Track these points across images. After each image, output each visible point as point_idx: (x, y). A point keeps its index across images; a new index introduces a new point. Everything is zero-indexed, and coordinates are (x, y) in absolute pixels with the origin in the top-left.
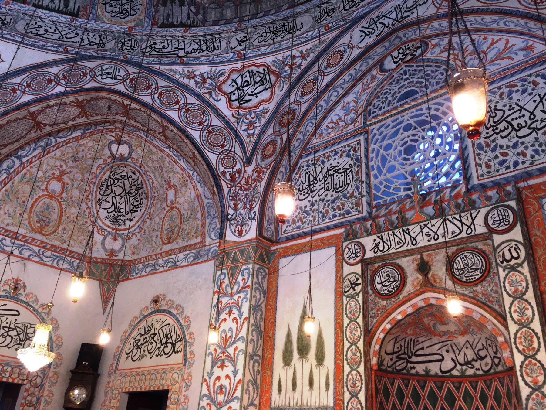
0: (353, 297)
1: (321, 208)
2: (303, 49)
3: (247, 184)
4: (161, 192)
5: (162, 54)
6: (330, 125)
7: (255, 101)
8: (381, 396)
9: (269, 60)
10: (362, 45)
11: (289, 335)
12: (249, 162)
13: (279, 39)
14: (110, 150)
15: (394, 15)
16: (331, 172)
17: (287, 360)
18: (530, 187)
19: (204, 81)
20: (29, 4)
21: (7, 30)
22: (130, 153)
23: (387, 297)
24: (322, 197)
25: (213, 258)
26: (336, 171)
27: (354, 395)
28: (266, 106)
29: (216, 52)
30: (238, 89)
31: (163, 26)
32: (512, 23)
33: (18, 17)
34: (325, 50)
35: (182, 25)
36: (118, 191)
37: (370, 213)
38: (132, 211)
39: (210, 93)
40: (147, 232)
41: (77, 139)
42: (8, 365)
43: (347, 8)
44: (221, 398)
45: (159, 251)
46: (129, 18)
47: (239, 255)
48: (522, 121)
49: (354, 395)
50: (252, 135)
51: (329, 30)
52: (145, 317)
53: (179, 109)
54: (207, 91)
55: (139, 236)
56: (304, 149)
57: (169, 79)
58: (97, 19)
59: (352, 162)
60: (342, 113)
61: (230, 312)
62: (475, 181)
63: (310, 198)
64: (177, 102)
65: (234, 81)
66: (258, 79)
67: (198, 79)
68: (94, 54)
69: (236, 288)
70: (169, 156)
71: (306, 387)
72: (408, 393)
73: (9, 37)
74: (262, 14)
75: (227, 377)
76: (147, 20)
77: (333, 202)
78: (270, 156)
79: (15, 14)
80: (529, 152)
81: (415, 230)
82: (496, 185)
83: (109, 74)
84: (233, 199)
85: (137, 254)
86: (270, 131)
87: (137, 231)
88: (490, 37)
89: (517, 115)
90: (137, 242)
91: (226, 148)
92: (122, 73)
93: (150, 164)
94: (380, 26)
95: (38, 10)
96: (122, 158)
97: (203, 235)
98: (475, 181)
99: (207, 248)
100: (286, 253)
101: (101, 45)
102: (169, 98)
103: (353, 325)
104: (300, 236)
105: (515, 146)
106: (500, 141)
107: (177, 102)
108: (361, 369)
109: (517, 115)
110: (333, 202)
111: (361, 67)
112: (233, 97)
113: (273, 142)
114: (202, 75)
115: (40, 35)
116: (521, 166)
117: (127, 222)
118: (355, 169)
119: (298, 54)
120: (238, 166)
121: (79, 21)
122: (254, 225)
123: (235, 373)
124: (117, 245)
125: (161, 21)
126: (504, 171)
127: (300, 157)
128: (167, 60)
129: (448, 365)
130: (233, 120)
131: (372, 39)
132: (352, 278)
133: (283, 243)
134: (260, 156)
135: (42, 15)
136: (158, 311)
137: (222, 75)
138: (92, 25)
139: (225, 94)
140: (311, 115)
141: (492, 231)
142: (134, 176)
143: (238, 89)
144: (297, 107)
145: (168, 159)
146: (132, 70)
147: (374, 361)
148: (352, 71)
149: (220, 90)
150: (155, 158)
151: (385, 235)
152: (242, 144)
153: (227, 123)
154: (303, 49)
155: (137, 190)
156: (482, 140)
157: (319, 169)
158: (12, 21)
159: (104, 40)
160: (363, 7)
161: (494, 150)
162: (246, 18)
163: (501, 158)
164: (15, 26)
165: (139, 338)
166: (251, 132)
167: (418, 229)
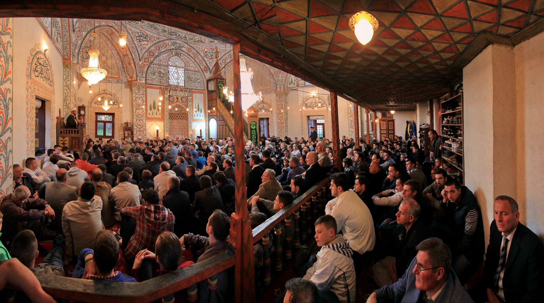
7: (143, 43)
9: (148, 33)
11: (151, 105)
12: (140, 60)
23: (172, 102)
32: (195, 63)
34: (163, 41)
44: (140, 116)
47: (140, 86)
51: (164, 36)
60: (162, 58)
61: (139, 99)
62: (186, 87)
66: (144, 36)
69: (140, 94)
71: (156, 115)
81: (178, 92)
82: (188, 89)
86: (146, 54)
88: (191, 62)
98: (186, 87)
100: (149, 87)
104: (152, 84)
123: (143, 112)
129: (173, 112)
130: (137, 46)
131: (174, 47)
134: (144, 60)
152: (139, 54)
157: (156, 70)
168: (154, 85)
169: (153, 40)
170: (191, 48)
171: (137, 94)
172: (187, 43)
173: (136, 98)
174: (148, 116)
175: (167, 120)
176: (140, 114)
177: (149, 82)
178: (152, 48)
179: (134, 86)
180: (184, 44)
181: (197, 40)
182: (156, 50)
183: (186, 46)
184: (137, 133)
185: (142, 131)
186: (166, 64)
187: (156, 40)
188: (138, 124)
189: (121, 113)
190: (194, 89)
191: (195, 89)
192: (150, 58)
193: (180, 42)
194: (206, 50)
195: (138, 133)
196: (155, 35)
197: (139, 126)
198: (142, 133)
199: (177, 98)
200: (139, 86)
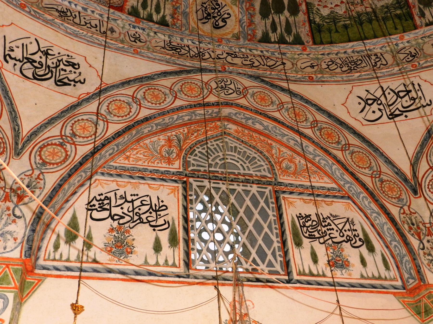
20: (421, 27)
21: (422, 59)
33: (418, 44)
73: (429, 64)
79: (414, 43)
158: (417, 50)
164: (424, 53)
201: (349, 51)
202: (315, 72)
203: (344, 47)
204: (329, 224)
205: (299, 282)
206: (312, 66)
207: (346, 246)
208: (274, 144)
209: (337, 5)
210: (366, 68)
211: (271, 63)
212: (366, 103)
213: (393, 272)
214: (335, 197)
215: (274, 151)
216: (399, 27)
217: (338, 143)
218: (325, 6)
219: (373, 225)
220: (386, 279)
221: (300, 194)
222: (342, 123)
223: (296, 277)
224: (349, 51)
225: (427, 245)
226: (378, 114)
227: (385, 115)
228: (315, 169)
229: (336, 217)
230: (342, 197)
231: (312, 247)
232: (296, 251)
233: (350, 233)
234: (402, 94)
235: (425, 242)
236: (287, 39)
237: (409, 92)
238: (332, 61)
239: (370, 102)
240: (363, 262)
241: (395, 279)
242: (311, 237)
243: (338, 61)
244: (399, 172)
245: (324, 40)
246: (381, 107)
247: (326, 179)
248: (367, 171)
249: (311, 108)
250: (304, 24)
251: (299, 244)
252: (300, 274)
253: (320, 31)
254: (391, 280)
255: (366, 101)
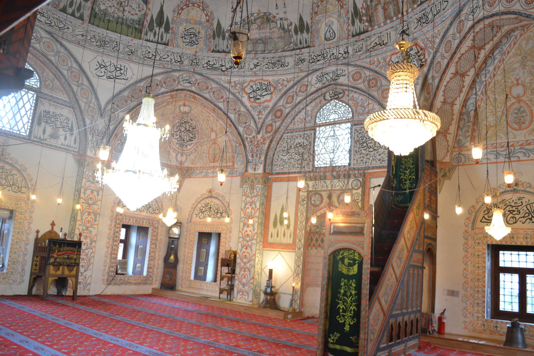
0: (303, 205)
1: (292, 162)
2: (289, 77)
3: (258, 144)
4: (207, 132)
5: (213, 68)
6: (299, 120)
7: (262, 99)
8: (310, 241)
9: (270, 79)
10: (316, 86)
11: (276, 216)
12: (259, 133)
13: (276, 69)
14: (180, 109)
15: (331, 76)
16: (298, 145)
17: (275, 225)
18: (369, 173)
19: (236, 86)
22: (190, 110)
24: (293, 157)
25: (239, 176)
26: (301, 146)
27: (300, 240)
28: (268, 104)
29: (242, 70)
30: (253, 91)
31: (213, 51)
33: (138, 47)
34: (299, 81)
35: (224, 52)
36: (183, 129)
37: (313, 170)
38: (190, 140)
39: (239, 92)
40: (199, 152)
41: (164, 106)
42: (144, 219)
43: (311, 62)
44: (248, 239)
45: (208, 165)
46: (195, 46)
48: (371, 145)
49: (300, 240)
50: (261, 118)
51: (301, 71)
52: (204, 198)
53: (223, 102)
54: (237, 91)
55: (195, 154)
56: (286, 129)
57: (217, 83)
58: (178, 46)
59: (308, 143)
62: (352, 166)
63: (287, 156)
64: (222, 98)
65: (252, 87)
66: (264, 88)
67: (233, 84)
68: (179, 69)
70: (213, 116)
71: (282, 236)
72: (320, 239)
73: (135, 61)
74: (267, 52)
75: (250, 231)
76: (205, 47)
77: (298, 160)
78: (270, 132)
80: (371, 159)
82: (358, 169)
83: (186, 80)
84: (251, 152)
85: (195, 165)
86: (270, 118)
87: (194, 151)
89: (370, 142)
90: (194, 158)
91: (247, 124)
92: (194, 80)
93: (201, 117)
94: (325, 79)
95: (148, 43)
96: (185, 113)
97: (233, 163)
99: (236, 169)
100: (276, 180)
101: (181, 62)
102: (218, 95)
103: (302, 216)
104: (282, 174)
105: (367, 155)
106: (364, 152)
107: (222, 98)
108: (303, 232)
109: (370, 142)
110: (298, 160)
111: (316, 95)
112: (251, 96)
113: (271, 125)
114: (235, 82)
115: (150, 58)
116: (367, 164)
117: (188, 146)
118: (308, 147)
119: (285, 79)
120: (253, 134)
121: (169, 48)
122: (262, 166)
123: (254, 230)
124: (184, 159)
125: (212, 49)
126: (362, 164)
127: (284, 133)
128: (216, 73)
130: (250, 109)
132: (303, 197)
133: (274, 175)
134: (264, 131)
135: (150, 46)
136: (211, 197)
137: (245, 82)
138: (176, 50)
139: (247, 93)
140: (290, 115)
141: (353, 188)
142: (191, 122)
143: (253, 91)
144: (283, 109)
145: (212, 118)
146: (198, 77)
147: (308, 229)
148: (311, 97)
149: (244, 91)
150: (204, 115)
151: (317, 182)
152: (255, 122)
153: (248, 110)
154: (289, 77)
155: (193, 129)
156: (357, 149)
159: (182, 59)
160: (318, 64)
161: (360, 154)
162: (259, 52)
163: (362, 159)
165: (202, 208)
166: (260, 116)
167: (329, 182)
168: (285, 173)
169: (281, 87)
170: (359, 69)
171: (248, 197)
172: (348, 64)
173: (246, 205)
174: (270, 240)
175: (299, 249)
176: (248, 235)
177: (277, 169)
178: (281, 103)
179: (245, 182)
180: (344, 68)
181: (373, 44)
182: (287, 103)
183: (351, 69)
184: (240, 273)
185: (249, 269)
186: (312, 124)
187: (286, 86)
188: (244, 254)
189: (230, 232)
190: (373, 168)
191: (377, 168)
192: (275, 122)
193: (334, 68)
194: (394, 57)
195: (242, 273)
196: (283, 77)
197: (245, 258)
198: (248, 273)
199: (330, 197)
200: (252, 182)
201: (105, 34)
202: (83, 40)
203: (103, 31)
204: (57, 118)
205: (33, 141)
206: (83, 36)
207: (61, 130)
208: (47, 70)
209: (110, 6)
210: (108, 48)
211: (61, 25)
212: (100, 66)
213: (77, 145)
214: (66, 106)
215: (45, 74)
216: (134, 34)
217: (78, 82)
218: (104, 4)
219: (77, 123)
220: (72, 147)
221: (50, 100)
222: (84, 72)
223: (32, 138)
224: (105, 34)
225: (94, 139)
226: (103, 74)
227: (105, 76)
228: (62, 89)
229: (62, 115)
230: (69, 107)
231: (45, 127)
232: (37, 127)
233: (65, 124)
234: (118, 69)
235: (94, 138)
236: (76, 14)
237: (121, 69)
238: (94, 36)
239: (102, 66)
240: (65, 138)
241: (76, 148)
242: (47, 122)
243: (97, 38)
244: (99, 105)
245: (95, 23)
246: (106, 71)
247: (66, 96)
248: (85, 100)
249: (72, 59)
250: (89, 9)
251: (39, 124)
252: (35, 137)
253: (95, 17)
254: (74, 148)
255: (100, 65)
